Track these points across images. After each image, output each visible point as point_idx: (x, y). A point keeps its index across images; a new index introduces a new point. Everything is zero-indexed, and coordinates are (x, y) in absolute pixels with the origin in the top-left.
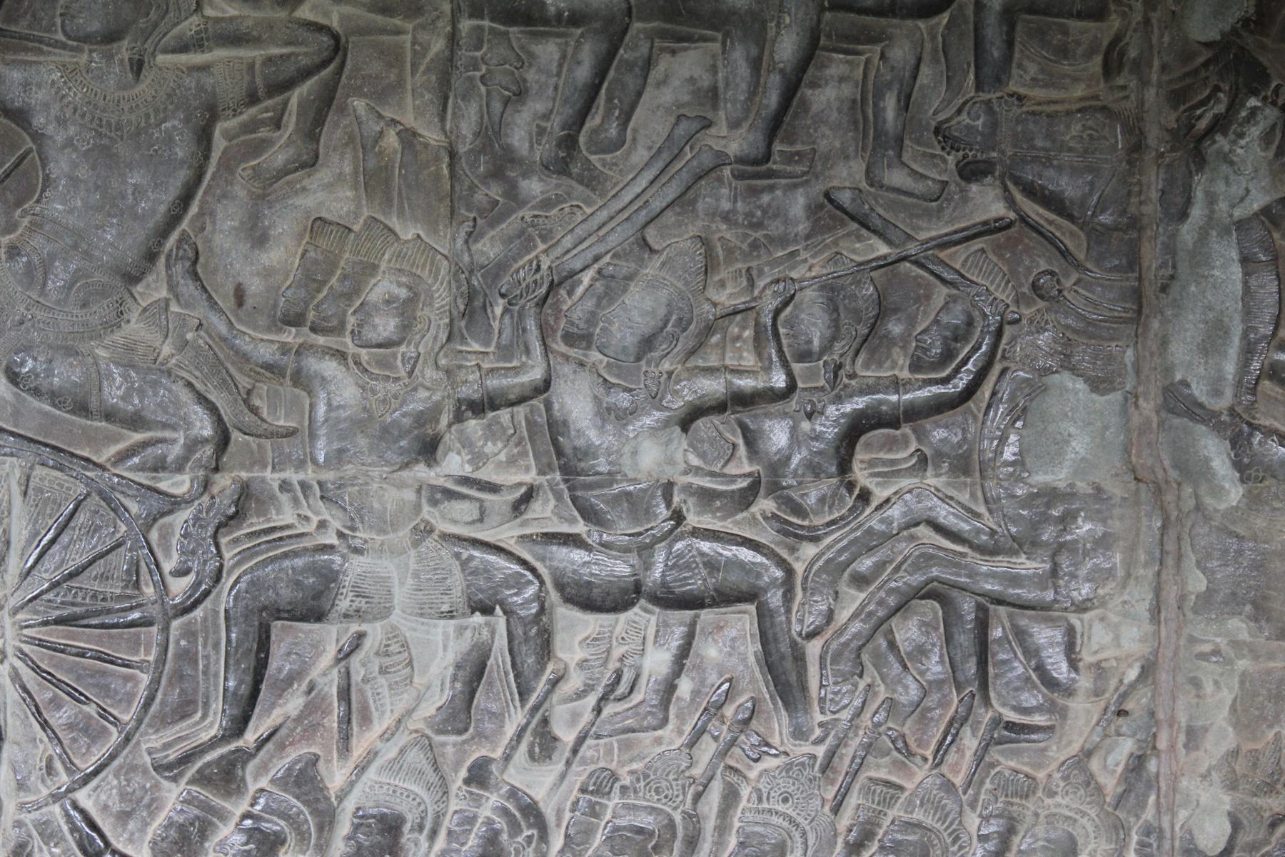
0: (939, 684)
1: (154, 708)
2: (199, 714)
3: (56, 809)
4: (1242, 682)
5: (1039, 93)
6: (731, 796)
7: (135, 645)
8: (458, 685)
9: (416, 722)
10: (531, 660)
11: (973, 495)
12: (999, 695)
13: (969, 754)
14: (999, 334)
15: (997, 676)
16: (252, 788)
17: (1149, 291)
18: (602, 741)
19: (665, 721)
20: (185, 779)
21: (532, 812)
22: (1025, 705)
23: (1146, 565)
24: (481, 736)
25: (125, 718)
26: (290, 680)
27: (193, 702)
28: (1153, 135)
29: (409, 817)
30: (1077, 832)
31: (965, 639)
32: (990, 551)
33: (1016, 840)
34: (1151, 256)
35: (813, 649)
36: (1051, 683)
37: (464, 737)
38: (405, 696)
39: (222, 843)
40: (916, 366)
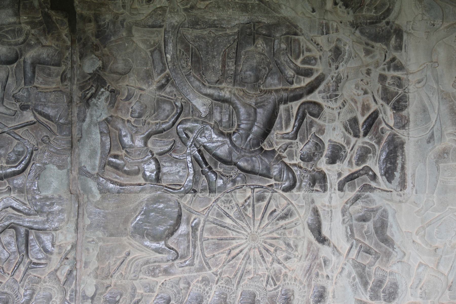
0: (14, 253)
4: (100, 249)
5: (43, 86)
11: (25, 199)
12: (31, 255)
13: (22, 272)
14: (32, 153)
15: (31, 250)
17: (75, 141)
22: (39, 257)
23: (73, 218)
28: (75, 98)
30: (52, 293)
31: (22, 240)
32: (28, 214)
33: (35, 296)
34: (75, 131)
36: (46, 251)
40: (8, 163)
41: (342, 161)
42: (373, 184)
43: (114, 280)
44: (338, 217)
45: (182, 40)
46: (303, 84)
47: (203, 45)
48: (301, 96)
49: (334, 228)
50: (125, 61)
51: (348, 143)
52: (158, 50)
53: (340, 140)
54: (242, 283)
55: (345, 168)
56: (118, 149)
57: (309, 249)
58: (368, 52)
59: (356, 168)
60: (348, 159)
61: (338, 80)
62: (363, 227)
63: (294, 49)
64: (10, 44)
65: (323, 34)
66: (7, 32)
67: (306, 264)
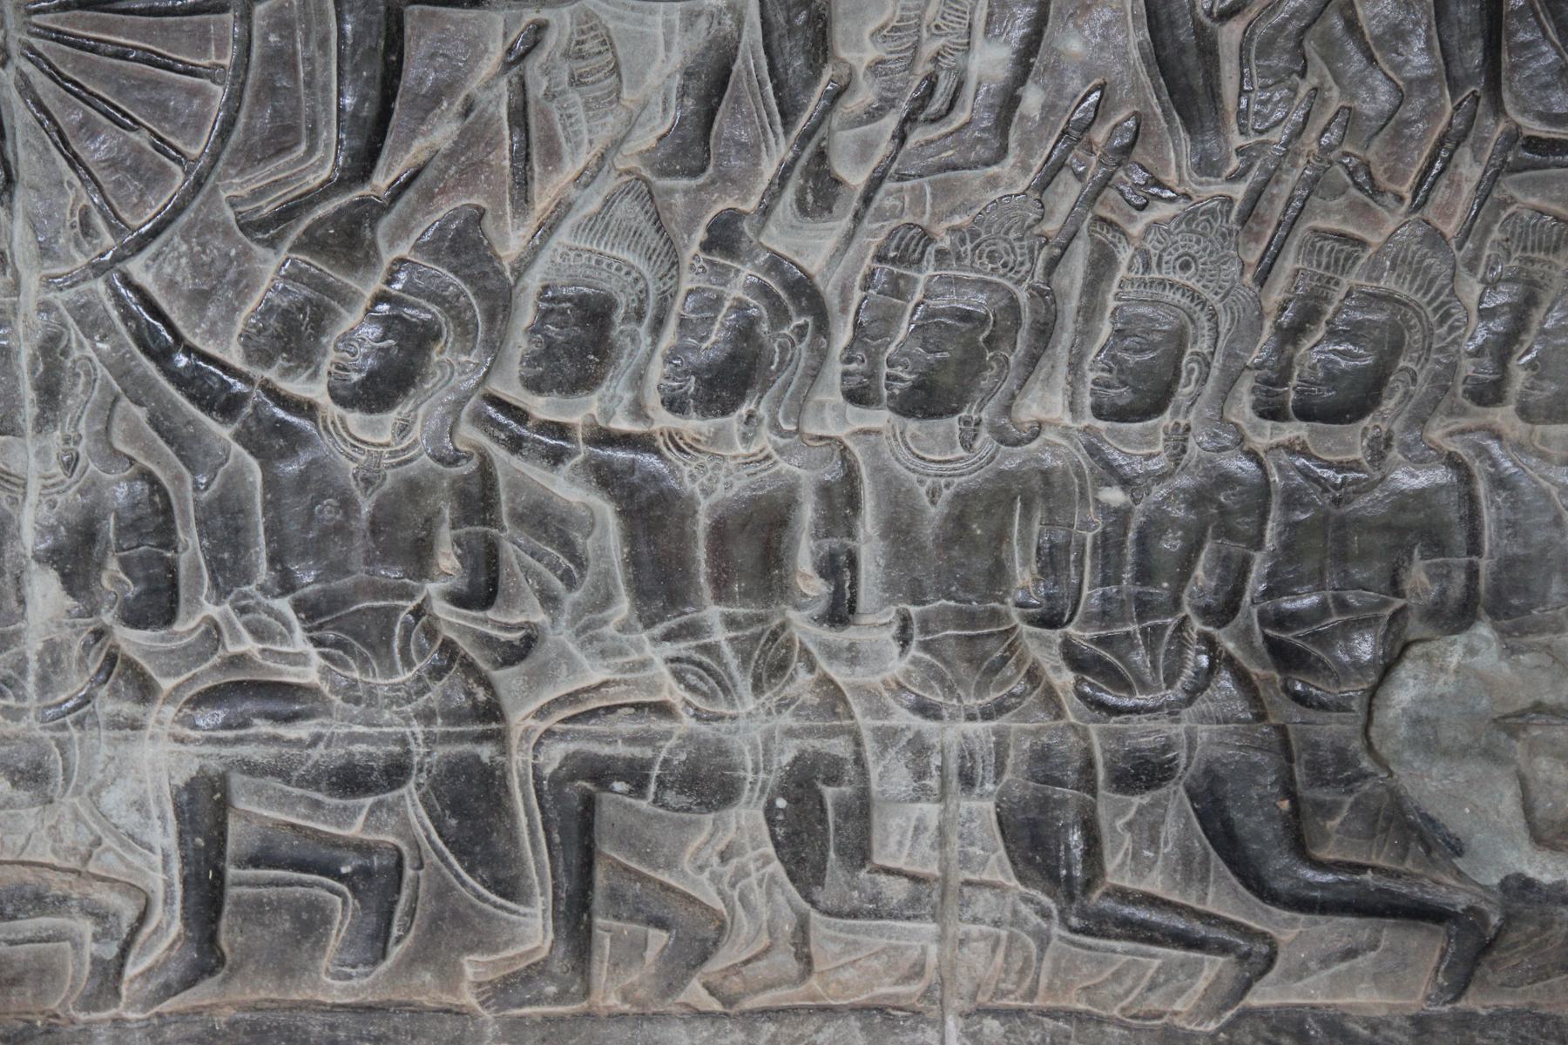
0: (1424, 83)
1: (236, 137)
2: (303, 147)
3: (100, 285)
6: (1103, 263)
7: (201, 42)
8: (689, 103)
9: (627, 159)
10: (798, 63)
12: (1517, 97)
13: (1467, 189)
15: (1515, 68)
16: (387, 257)
18: (907, 184)
19: (1002, 153)
20: (288, 244)
21: (804, 291)
22: (1557, 110)
24: (725, 179)
25: (194, 151)
26: (436, 97)
27: (292, 129)
29: (622, 299)
33: (1537, 315)
35: (1230, 35)
37: (701, 180)
38: (610, 119)
39: (347, 338)
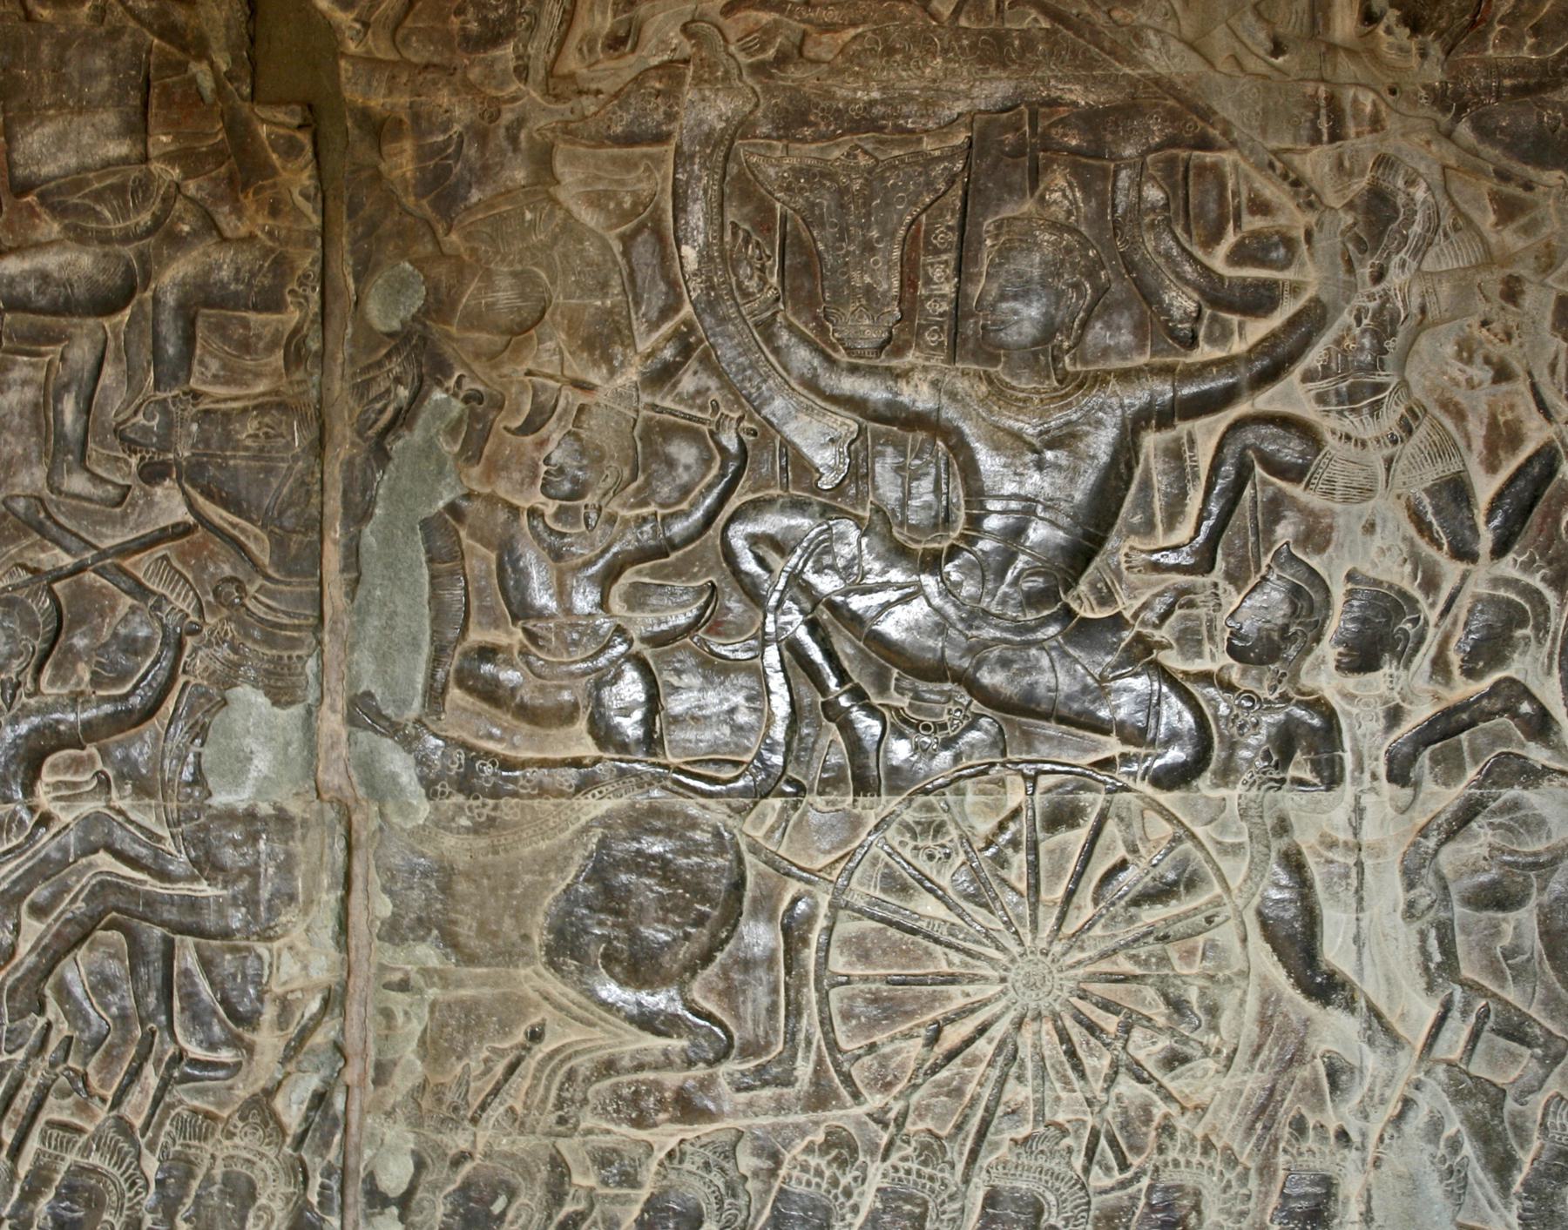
4: (432, 1012)
5: (220, 391)
11: (158, 818)
14: (180, 646)
23: (331, 887)
30: (256, 1175)
31: (152, 973)
41: (1405, 658)
42: (1538, 755)
43: (484, 1135)
44: (1388, 891)
45: (746, 188)
46: (1238, 347)
47: (826, 201)
48: (1226, 397)
49: (1372, 936)
50: (524, 279)
51: (1430, 584)
52: (652, 230)
53: (1400, 576)
54: (985, 1160)
55: (1416, 689)
56: (496, 623)
57: (1265, 1022)
58: (1508, 210)
59: (1464, 689)
60: (1428, 650)
61: (1384, 326)
62: (1495, 931)
63: (1198, 206)
64: (105, 239)
65: (1315, 140)
66: (98, 196)
67: (1253, 1082)
